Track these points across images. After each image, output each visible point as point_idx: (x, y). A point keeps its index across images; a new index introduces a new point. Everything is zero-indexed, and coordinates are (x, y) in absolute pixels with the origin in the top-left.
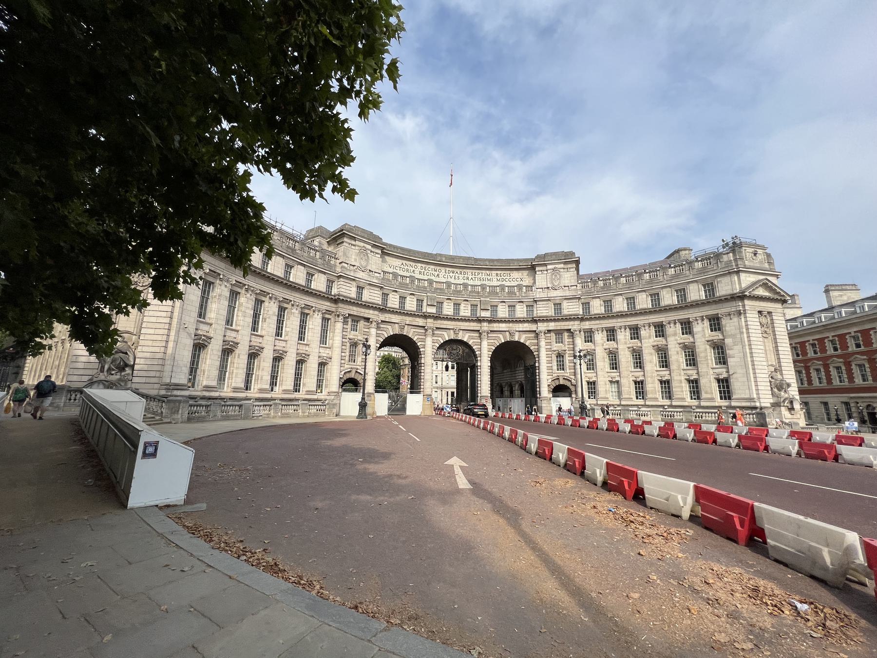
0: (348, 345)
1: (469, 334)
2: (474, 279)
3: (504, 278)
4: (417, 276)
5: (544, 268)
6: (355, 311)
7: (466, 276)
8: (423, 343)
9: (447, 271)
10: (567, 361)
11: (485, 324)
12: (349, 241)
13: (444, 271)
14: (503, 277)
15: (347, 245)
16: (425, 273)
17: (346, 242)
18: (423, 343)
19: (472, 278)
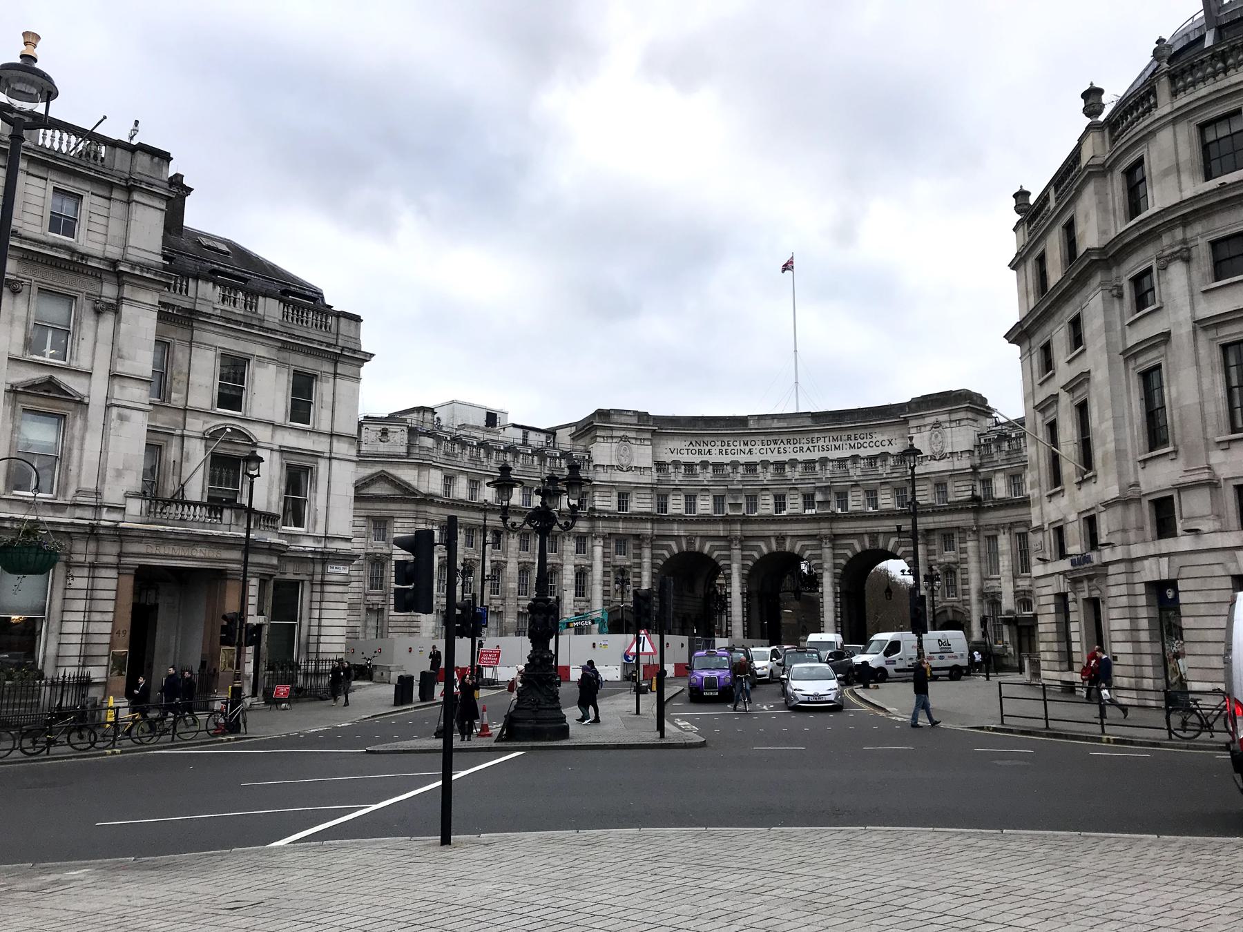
0: (612, 574)
1: (803, 543)
2: (812, 449)
3: (862, 442)
4: (715, 458)
5: (921, 422)
6: (621, 527)
7: (798, 445)
8: (728, 562)
9: (765, 442)
10: (959, 582)
11: (826, 525)
12: (603, 434)
13: (760, 443)
14: (859, 441)
15: (602, 440)
16: (729, 451)
17: (600, 436)
18: (728, 562)
19: (808, 449)
